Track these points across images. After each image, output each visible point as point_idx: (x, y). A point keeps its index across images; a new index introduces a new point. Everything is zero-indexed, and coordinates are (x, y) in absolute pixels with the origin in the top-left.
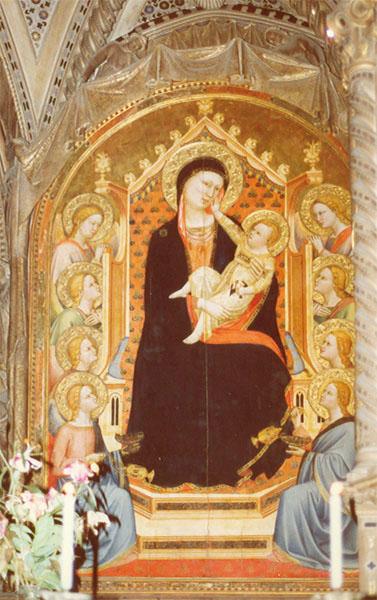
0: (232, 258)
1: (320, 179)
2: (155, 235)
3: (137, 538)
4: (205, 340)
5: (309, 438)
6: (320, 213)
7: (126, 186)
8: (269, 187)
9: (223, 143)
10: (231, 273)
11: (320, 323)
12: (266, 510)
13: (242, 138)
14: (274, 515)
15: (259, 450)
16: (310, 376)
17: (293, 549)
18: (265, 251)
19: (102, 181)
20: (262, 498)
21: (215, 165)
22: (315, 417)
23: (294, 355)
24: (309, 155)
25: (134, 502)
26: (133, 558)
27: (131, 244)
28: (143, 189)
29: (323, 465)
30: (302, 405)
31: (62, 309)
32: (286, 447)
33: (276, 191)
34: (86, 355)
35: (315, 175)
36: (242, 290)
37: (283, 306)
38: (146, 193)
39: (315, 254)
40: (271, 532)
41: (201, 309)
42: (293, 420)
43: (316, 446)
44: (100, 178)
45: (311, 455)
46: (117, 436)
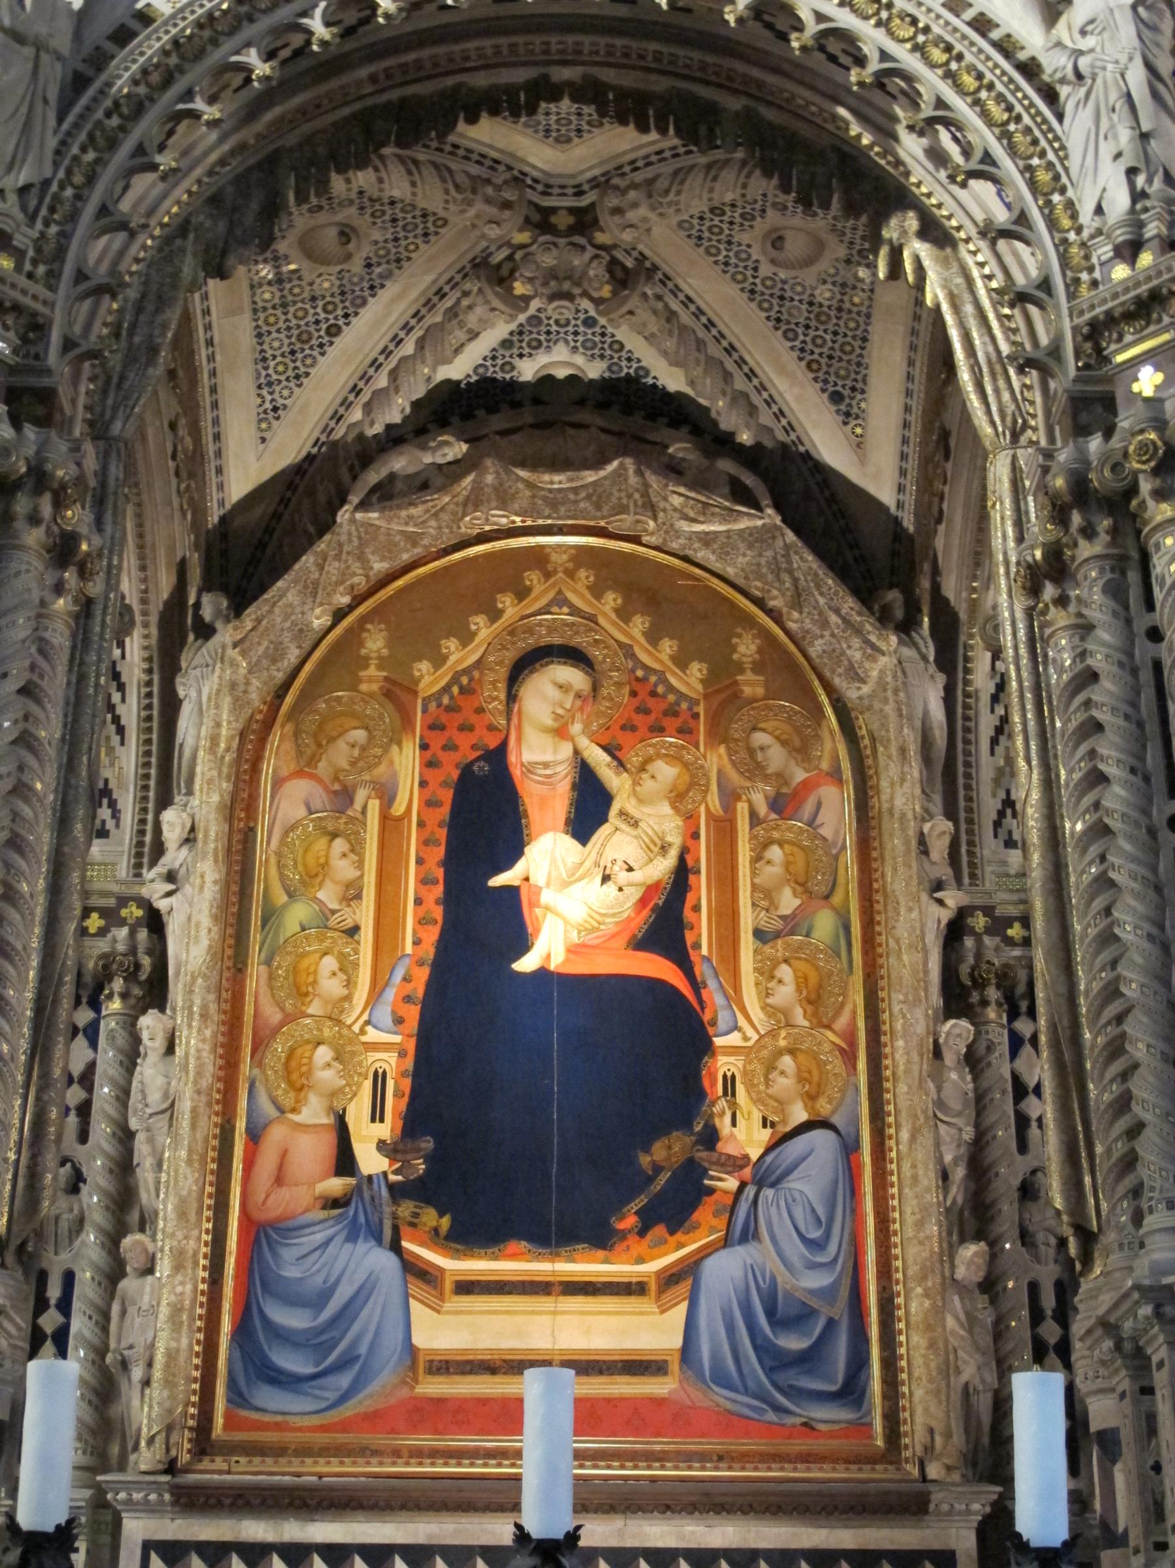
0: (603, 819)
1: (760, 691)
2: (466, 770)
3: (411, 1351)
4: (552, 967)
5: (746, 1157)
6: (762, 749)
7: (417, 681)
8: (671, 698)
9: (592, 619)
10: (603, 845)
11: (765, 942)
12: (667, 1297)
13: (624, 614)
14: (683, 1307)
15: (650, 1180)
16: (746, 1039)
17: (720, 1378)
18: (666, 809)
19: (372, 671)
20: (658, 1273)
21: (574, 656)
22: (757, 1116)
23: (719, 1000)
24: (742, 649)
25: (409, 1278)
26: (404, 1393)
27: (423, 784)
28: (446, 689)
29: (773, 1210)
30: (734, 1094)
31: (285, 898)
32: (704, 1173)
33: (684, 706)
34: (331, 986)
35: (751, 685)
36: (623, 877)
37: (697, 908)
38: (452, 697)
39: (754, 819)
40: (677, 1342)
41: (547, 908)
42: (717, 1121)
43: (765, 1176)
44: (367, 667)
45: (750, 1191)
46: (381, 1146)
